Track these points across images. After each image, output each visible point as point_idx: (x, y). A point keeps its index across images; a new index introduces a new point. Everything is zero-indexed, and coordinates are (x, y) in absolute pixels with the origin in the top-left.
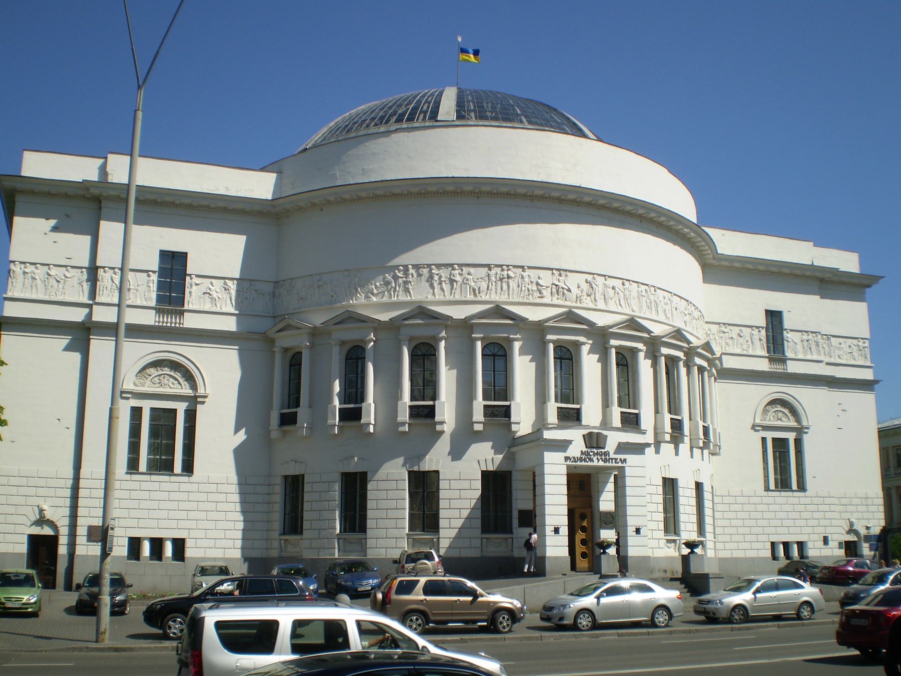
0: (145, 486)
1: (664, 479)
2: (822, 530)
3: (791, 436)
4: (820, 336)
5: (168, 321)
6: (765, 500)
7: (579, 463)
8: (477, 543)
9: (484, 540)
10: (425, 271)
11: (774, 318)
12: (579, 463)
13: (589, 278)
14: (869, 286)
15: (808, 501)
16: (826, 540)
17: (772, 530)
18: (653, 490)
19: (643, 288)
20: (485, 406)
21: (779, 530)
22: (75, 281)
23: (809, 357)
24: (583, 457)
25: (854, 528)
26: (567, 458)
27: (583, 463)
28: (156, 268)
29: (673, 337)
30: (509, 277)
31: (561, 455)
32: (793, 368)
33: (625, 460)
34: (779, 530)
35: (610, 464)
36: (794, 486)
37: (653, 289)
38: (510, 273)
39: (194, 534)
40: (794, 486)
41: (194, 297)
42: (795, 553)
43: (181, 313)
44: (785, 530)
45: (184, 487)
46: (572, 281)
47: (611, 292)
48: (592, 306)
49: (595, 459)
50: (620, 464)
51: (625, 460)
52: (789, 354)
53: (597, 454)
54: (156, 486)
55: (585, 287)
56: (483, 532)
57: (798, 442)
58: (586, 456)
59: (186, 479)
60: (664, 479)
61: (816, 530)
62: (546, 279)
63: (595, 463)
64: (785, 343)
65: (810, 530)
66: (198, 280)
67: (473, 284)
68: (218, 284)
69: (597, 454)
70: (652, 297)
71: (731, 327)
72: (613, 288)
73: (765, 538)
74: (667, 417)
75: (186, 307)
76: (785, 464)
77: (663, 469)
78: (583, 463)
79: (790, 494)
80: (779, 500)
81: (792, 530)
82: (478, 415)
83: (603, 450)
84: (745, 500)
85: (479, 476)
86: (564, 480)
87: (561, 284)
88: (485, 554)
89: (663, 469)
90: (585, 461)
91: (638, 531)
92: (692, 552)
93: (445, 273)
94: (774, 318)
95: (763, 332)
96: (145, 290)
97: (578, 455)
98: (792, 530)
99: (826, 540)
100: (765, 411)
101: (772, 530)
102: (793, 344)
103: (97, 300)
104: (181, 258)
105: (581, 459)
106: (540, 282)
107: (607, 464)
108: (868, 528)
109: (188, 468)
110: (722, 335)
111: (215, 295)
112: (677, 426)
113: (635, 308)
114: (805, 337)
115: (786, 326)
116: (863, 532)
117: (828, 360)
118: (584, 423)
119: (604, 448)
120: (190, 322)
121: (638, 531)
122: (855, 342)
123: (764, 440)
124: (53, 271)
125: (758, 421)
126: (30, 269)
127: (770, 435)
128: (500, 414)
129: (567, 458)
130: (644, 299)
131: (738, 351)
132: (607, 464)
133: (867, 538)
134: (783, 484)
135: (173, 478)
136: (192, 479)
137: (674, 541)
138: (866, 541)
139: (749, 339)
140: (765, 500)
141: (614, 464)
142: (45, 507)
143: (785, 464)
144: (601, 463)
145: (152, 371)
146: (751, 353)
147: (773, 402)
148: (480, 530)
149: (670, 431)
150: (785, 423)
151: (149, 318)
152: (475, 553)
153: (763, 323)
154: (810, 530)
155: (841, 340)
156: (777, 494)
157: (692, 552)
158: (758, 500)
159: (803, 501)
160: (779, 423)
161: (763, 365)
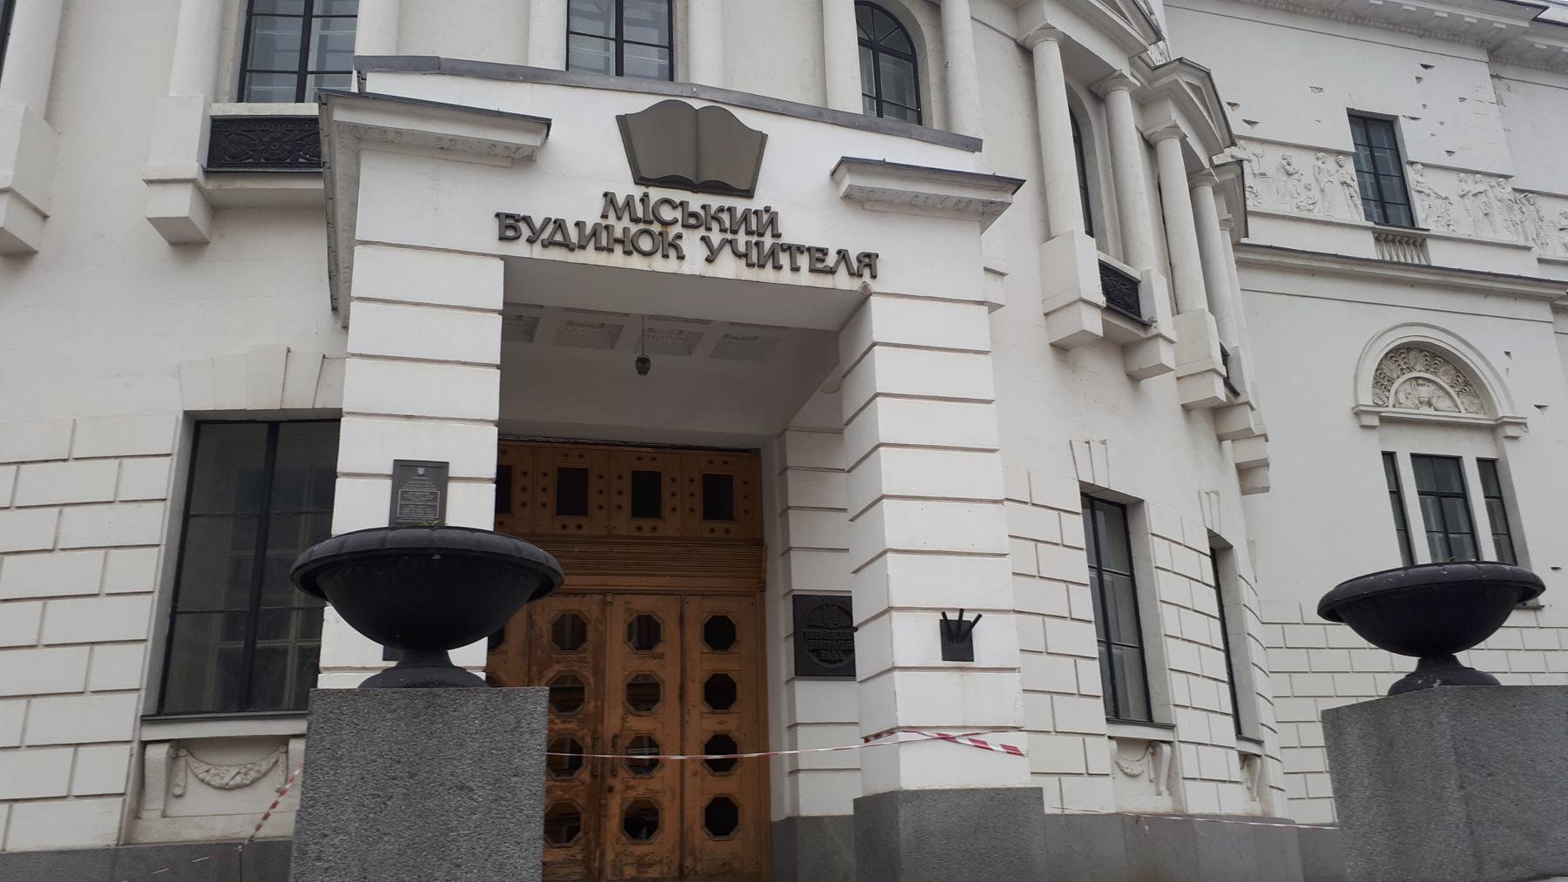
3: (1470, 450)
7: (590, 256)
8: (113, 770)
9: (157, 754)
11: (1375, 133)
12: (590, 256)
26: (510, 225)
27: (617, 259)
31: (464, 206)
33: (869, 261)
35: (786, 277)
50: (843, 281)
51: (869, 261)
56: (161, 709)
63: (694, 261)
64: (1416, 198)
69: (693, 221)
77: (1081, 451)
78: (617, 259)
83: (740, 205)
86: (487, 338)
88: (155, 830)
89: (1081, 451)
90: (631, 248)
94: (1375, 133)
95: (1350, 166)
97: (592, 218)
105: (594, 237)
107: (768, 275)
114: (1471, 185)
119: (748, 194)
123: (1389, 457)
125: (1367, 398)
127: (1406, 445)
129: (510, 225)
132: (768, 275)
139: (1308, 178)
141: (805, 278)
144: (728, 267)
146: (1316, 214)
147: (1399, 353)
150: (1444, 408)
152: (94, 827)
161: (1364, 246)
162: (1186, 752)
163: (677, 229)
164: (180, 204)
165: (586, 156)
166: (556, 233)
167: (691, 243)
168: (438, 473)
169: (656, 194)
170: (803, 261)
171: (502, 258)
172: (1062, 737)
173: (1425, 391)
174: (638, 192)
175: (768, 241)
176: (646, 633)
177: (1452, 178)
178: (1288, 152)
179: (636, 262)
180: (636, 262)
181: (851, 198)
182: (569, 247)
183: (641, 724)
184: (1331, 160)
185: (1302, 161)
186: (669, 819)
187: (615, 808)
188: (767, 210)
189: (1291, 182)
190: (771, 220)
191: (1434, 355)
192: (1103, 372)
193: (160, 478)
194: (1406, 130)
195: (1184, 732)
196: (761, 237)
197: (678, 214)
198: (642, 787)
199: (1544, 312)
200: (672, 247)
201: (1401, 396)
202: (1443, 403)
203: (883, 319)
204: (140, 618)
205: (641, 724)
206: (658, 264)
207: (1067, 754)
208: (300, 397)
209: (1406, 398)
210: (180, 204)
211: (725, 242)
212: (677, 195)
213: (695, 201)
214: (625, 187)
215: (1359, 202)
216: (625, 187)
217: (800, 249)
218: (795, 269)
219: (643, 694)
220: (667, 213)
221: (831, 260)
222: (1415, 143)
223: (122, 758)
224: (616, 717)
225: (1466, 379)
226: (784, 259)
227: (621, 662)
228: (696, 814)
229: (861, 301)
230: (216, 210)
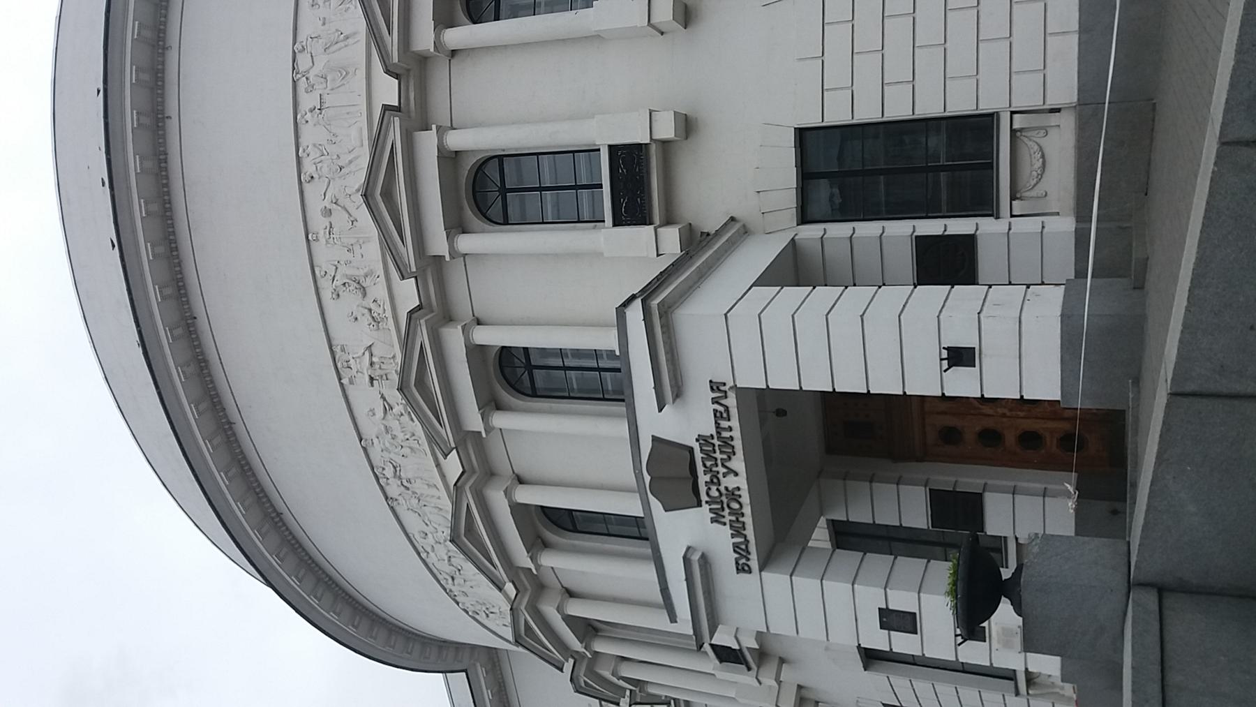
7: (750, 532)
12: (750, 532)
13: (327, 295)
24: (728, 518)
26: (742, 569)
27: (748, 519)
33: (715, 386)
35: (736, 433)
38: (389, 472)
50: (731, 401)
51: (715, 386)
55: (351, 300)
63: (741, 482)
69: (715, 480)
78: (748, 519)
83: (698, 456)
90: (739, 514)
91: (959, 357)
97: (727, 530)
105: (738, 530)
106: (380, 413)
107: (738, 443)
113: (354, 133)
119: (691, 450)
121: (959, 357)
129: (742, 569)
130: (329, 100)
132: (738, 443)
141: (735, 423)
144: (738, 463)
163: (722, 488)
166: (741, 550)
167: (730, 482)
169: (704, 498)
170: (724, 424)
171: (761, 570)
172: (1014, 29)
174: (706, 507)
175: (716, 442)
179: (747, 510)
180: (747, 510)
181: (678, 394)
182: (747, 541)
188: (697, 440)
196: (716, 445)
197: (714, 488)
200: (733, 495)
203: (752, 379)
206: (745, 499)
211: (723, 465)
212: (703, 489)
213: (703, 478)
217: (718, 426)
218: (730, 429)
220: (714, 493)
221: (721, 409)
226: (725, 434)
229: (741, 392)
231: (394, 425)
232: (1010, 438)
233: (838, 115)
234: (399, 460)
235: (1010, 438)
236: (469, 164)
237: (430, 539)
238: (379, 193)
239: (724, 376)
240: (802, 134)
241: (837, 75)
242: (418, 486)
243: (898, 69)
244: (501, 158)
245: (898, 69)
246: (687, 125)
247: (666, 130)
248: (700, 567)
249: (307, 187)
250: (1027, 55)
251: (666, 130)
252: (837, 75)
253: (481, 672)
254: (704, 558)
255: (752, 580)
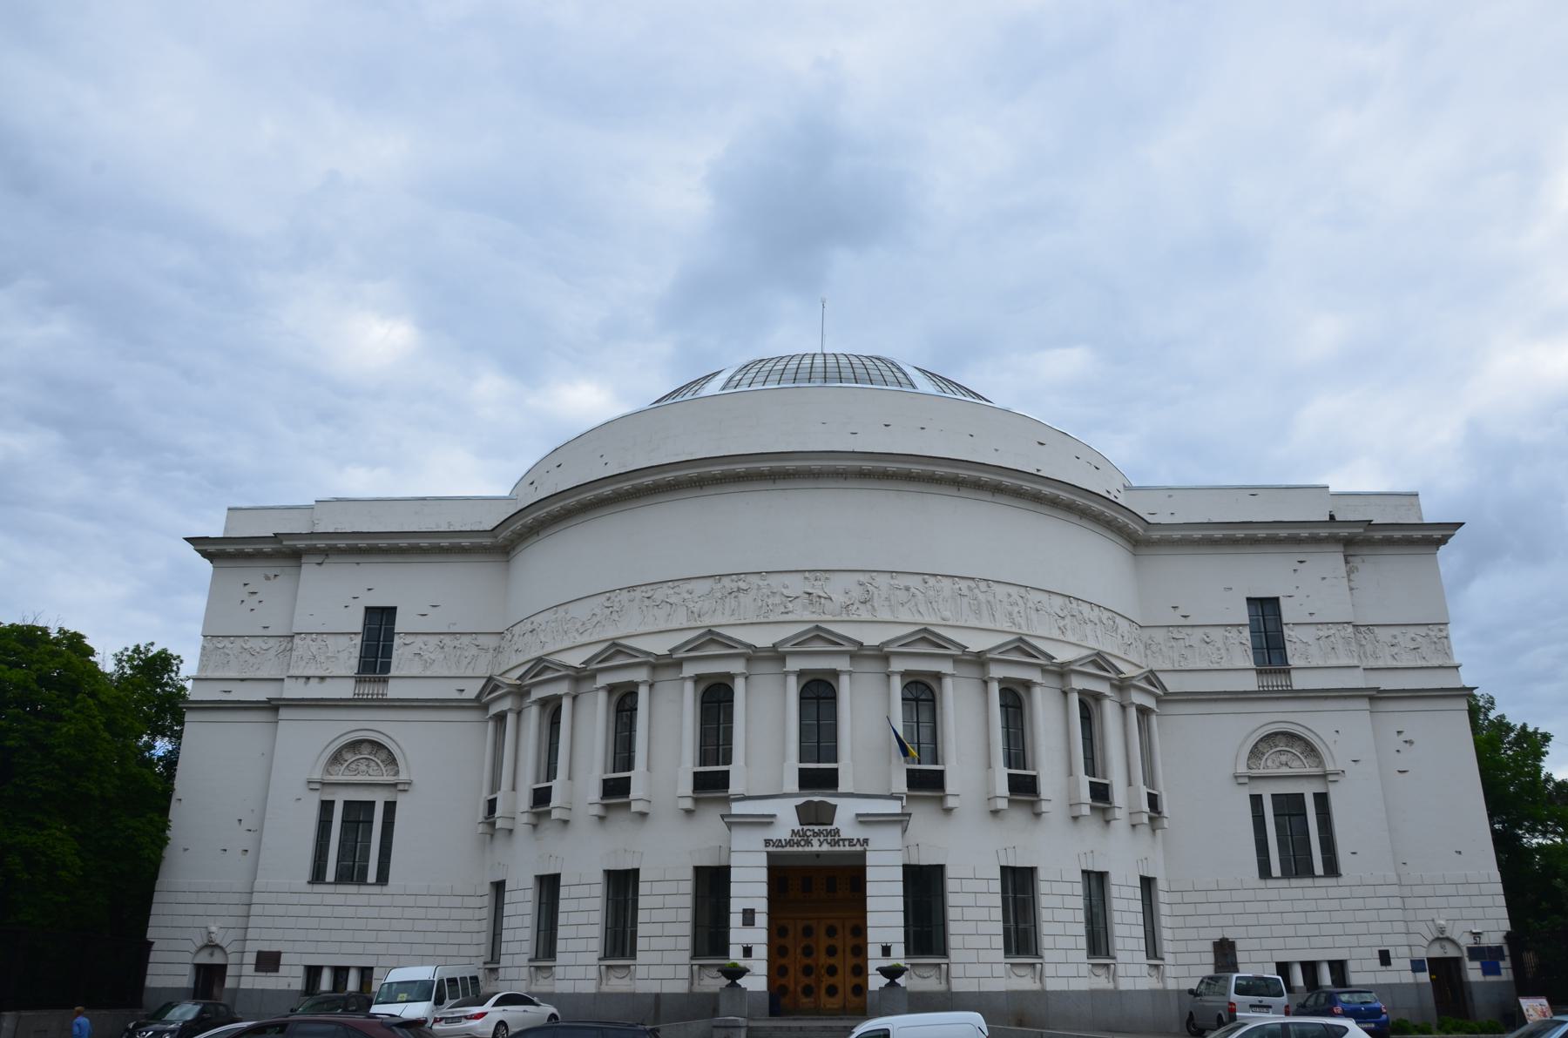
0: (329, 899)
1: (1003, 868)
2: (1376, 940)
3: (1308, 790)
4: (1350, 629)
5: (369, 690)
6: (1262, 895)
7: (788, 849)
8: (684, 972)
9: (695, 968)
10: (638, 594)
11: (1265, 610)
14: (1443, 541)
15: (1345, 892)
16: (1385, 958)
17: (1279, 943)
18: (1066, 888)
19: (964, 584)
20: (695, 774)
21: (1291, 943)
22: (272, 652)
23: (1334, 662)
25: (1447, 934)
26: (767, 842)
27: (795, 849)
28: (359, 629)
29: (1017, 649)
30: (739, 589)
32: (1299, 681)
33: (866, 841)
34: (1291, 943)
36: (1319, 868)
37: (983, 585)
38: (742, 585)
39: (383, 961)
40: (1319, 868)
41: (402, 658)
42: (1326, 978)
43: (385, 681)
44: (1304, 942)
45: (374, 900)
46: (837, 588)
47: (903, 596)
48: (870, 618)
49: (815, 842)
50: (858, 848)
51: (866, 841)
52: (1294, 661)
53: (816, 834)
54: (340, 899)
55: (857, 593)
56: (696, 954)
57: (1322, 800)
58: (800, 837)
59: (377, 889)
60: (1003, 868)
61: (1364, 940)
62: (796, 585)
63: (816, 847)
65: (1352, 941)
66: (409, 639)
67: (691, 605)
68: (434, 640)
69: (816, 834)
70: (982, 597)
71: (1189, 631)
72: (907, 589)
73: (1266, 956)
74: (1001, 774)
75: (393, 672)
76: (1296, 836)
77: (1002, 853)
78: (795, 849)
79: (1308, 882)
80: (1286, 894)
81: (1316, 942)
82: (686, 786)
84: (1225, 896)
85: (689, 874)
86: (763, 875)
87: (816, 592)
88: (697, 989)
89: (1002, 853)
90: (798, 844)
92: (892, 984)
93: (660, 594)
95: (1246, 632)
96: (348, 656)
98: (1316, 942)
99: (1385, 958)
100: (1255, 753)
101: (1279, 943)
102: (1300, 645)
103: (292, 673)
104: (390, 612)
105: (789, 843)
106: (786, 592)
107: (836, 848)
108: (1477, 935)
109: (383, 878)
110: (1173, 643)
111: (426, 656)
112: (1024, 787)
113: (947, 614)
114: (1324, 632)
115: (1285, 620)
116: (1466, 941)
117: (1365, 665)
118: (841, 789)
120: (395, 690)
122: (1423, 631)
123: (1256, 800)
124: (252, 643)
125: (1242, 769)
126: (226, 642)
127: (1267, 791)
128: (711, 784)
129: (767, 842)
130: (965, 600)
131: (1204, 666)
132: (836, 848)
133: (1475, 953)
134: (1298, 866)
135: (364, 889)
136: (385, 889)
137: (1107, 965)
138: (1472, 958)
139: (1219, 644)
140: (1262, 895)
141: (848, 848)
142: (213, 929)
143: (1296, 836)
144: (825, 847)
145: (350, 757)
148: (688, 954)
149: (1007, 794)
150: (1297, 768)
151: (346, 690)
152: (681, 987)
153: (1244, 618)
154: (1352, 941)
155: (1395, 631)
156: (1284, 883)
157: (892, 984)
158: (1250, 895)
159: (1333, 892)
160: (1284, 770)
161: (1250, 682)
162: (1047, 967)
164: (688, 804)
165: (787, 821)
168: (752, 911)
173: (1284, 758)
176: (831, 931)
177: (1313, 628)
178: (1207, 630)
183: (832, 961)
184: (1234, 630)
185: (1217, 634)
186: (841, 990)
187: (823, 987)
189: (1208, 649)
190: (837, 832)
191: (1291, 737)
192: (1019, 817)
193: (688, 887)
194: (1284, 603)
195: (1047, 959)
198: (831, 980)
199: (1365, 704)
200: (808, 843)
201: (1269, 763)
202: (1296, 763)
203: (870, 859)
204: (687, 929)
205: (832, 961)
207: (985, 970)
208: (724, 863)
209: (1269, 765)
210: (688, 804)
213: (816, 828)
214: (797, 827)
215: (1250, 653)
216: (797, 827)
219: (831, 951)
222: (1288, 613)
223: (687, 968)
224: (824, 960)
225: (1310, 750)
227: (824, 941)
228: (849, 990)
230: (696, 800)
231: (777, 600)
232: (783, 961)
233: (951, 885)
234: (753, 593)
235: (783, 961)
236: (934, 685)
237: (687, 596)
238: (927, 636)
239: (871, 846)
240: (941, 868)
241: (970, 886)
242: (731, 602)
243: (969, 913)
244: (933, 700)
245: (970, 914)
246: (948, 811)
247: (950, 802)
248: (767, 821)
249: (920, 578)
250: (973, 970)
251: (950, 802)
252: (970, 886)
253: (487, 541)
254: (771, 823)
255: (761, 846)
